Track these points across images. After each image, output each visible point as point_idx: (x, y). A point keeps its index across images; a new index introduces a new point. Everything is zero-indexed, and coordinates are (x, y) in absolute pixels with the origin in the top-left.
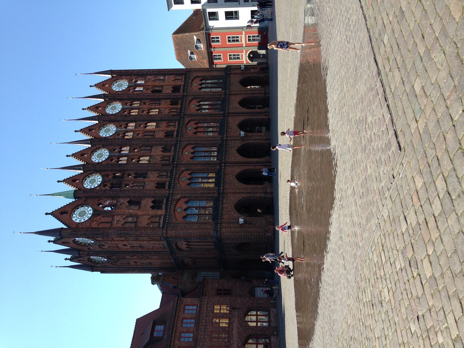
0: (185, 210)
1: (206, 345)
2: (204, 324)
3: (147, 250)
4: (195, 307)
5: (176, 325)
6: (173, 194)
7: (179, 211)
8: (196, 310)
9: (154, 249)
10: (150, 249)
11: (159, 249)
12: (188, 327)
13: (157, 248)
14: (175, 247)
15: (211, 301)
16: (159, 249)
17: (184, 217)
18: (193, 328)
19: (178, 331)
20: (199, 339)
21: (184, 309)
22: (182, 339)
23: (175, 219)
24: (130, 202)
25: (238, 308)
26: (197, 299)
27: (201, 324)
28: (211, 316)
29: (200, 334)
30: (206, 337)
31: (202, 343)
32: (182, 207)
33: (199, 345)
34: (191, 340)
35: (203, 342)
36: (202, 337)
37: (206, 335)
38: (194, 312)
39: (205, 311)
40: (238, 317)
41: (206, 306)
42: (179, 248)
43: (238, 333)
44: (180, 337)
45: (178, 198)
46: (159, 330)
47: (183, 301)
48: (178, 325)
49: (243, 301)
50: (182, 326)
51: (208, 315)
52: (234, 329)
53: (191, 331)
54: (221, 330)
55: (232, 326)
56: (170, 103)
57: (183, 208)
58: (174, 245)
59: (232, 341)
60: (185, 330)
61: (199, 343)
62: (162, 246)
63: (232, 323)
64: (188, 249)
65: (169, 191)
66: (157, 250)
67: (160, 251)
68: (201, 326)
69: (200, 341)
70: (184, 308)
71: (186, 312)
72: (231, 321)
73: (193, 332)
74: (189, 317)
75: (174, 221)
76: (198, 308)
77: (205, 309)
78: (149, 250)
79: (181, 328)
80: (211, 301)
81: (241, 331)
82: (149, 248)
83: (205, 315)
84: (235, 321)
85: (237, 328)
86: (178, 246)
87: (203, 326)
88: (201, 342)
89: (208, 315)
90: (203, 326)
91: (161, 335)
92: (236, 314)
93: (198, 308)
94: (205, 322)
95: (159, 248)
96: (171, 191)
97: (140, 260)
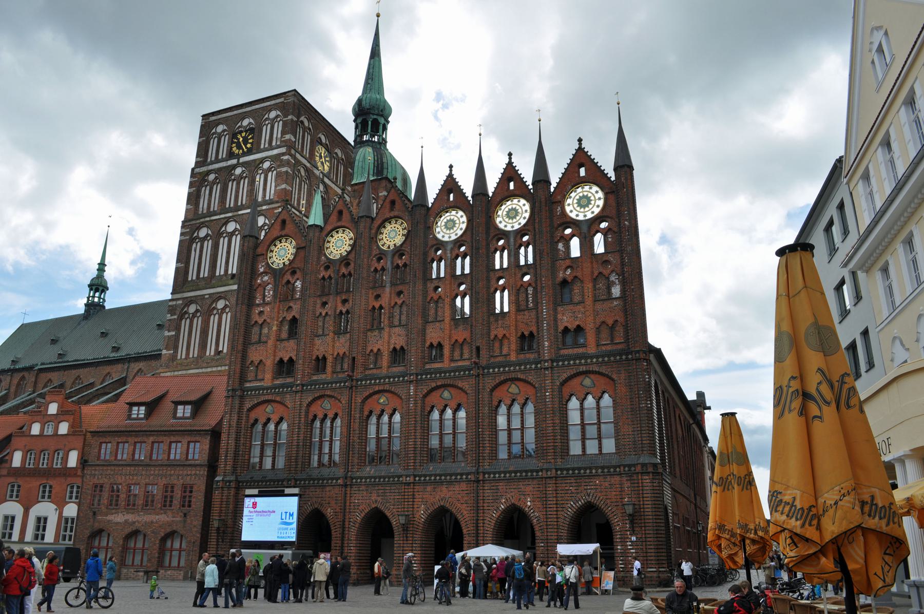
2: (169, 473)
4: (196, 457)
7: (267, 410)
15: (199, 479)
24: (294, 320)
25: (185, 521)
26: (207, 458)
27: (169, 469)
30: (152, 477)
33: (143, 470)
39: (185, 472)
40: (173, 521)
41: (194, 472)
44: (159, 442)
47: (206, 438)
48: (172, 437)
49: (195, 529)
51: (180, 477)
52: (157, 517)
55: (162, 514)
56: (526, 333)
59: (142, 513)
77: (189, 473)
80: (199, 479)
84: (168, 517)
92: (177, 519)
94: (171, 475)
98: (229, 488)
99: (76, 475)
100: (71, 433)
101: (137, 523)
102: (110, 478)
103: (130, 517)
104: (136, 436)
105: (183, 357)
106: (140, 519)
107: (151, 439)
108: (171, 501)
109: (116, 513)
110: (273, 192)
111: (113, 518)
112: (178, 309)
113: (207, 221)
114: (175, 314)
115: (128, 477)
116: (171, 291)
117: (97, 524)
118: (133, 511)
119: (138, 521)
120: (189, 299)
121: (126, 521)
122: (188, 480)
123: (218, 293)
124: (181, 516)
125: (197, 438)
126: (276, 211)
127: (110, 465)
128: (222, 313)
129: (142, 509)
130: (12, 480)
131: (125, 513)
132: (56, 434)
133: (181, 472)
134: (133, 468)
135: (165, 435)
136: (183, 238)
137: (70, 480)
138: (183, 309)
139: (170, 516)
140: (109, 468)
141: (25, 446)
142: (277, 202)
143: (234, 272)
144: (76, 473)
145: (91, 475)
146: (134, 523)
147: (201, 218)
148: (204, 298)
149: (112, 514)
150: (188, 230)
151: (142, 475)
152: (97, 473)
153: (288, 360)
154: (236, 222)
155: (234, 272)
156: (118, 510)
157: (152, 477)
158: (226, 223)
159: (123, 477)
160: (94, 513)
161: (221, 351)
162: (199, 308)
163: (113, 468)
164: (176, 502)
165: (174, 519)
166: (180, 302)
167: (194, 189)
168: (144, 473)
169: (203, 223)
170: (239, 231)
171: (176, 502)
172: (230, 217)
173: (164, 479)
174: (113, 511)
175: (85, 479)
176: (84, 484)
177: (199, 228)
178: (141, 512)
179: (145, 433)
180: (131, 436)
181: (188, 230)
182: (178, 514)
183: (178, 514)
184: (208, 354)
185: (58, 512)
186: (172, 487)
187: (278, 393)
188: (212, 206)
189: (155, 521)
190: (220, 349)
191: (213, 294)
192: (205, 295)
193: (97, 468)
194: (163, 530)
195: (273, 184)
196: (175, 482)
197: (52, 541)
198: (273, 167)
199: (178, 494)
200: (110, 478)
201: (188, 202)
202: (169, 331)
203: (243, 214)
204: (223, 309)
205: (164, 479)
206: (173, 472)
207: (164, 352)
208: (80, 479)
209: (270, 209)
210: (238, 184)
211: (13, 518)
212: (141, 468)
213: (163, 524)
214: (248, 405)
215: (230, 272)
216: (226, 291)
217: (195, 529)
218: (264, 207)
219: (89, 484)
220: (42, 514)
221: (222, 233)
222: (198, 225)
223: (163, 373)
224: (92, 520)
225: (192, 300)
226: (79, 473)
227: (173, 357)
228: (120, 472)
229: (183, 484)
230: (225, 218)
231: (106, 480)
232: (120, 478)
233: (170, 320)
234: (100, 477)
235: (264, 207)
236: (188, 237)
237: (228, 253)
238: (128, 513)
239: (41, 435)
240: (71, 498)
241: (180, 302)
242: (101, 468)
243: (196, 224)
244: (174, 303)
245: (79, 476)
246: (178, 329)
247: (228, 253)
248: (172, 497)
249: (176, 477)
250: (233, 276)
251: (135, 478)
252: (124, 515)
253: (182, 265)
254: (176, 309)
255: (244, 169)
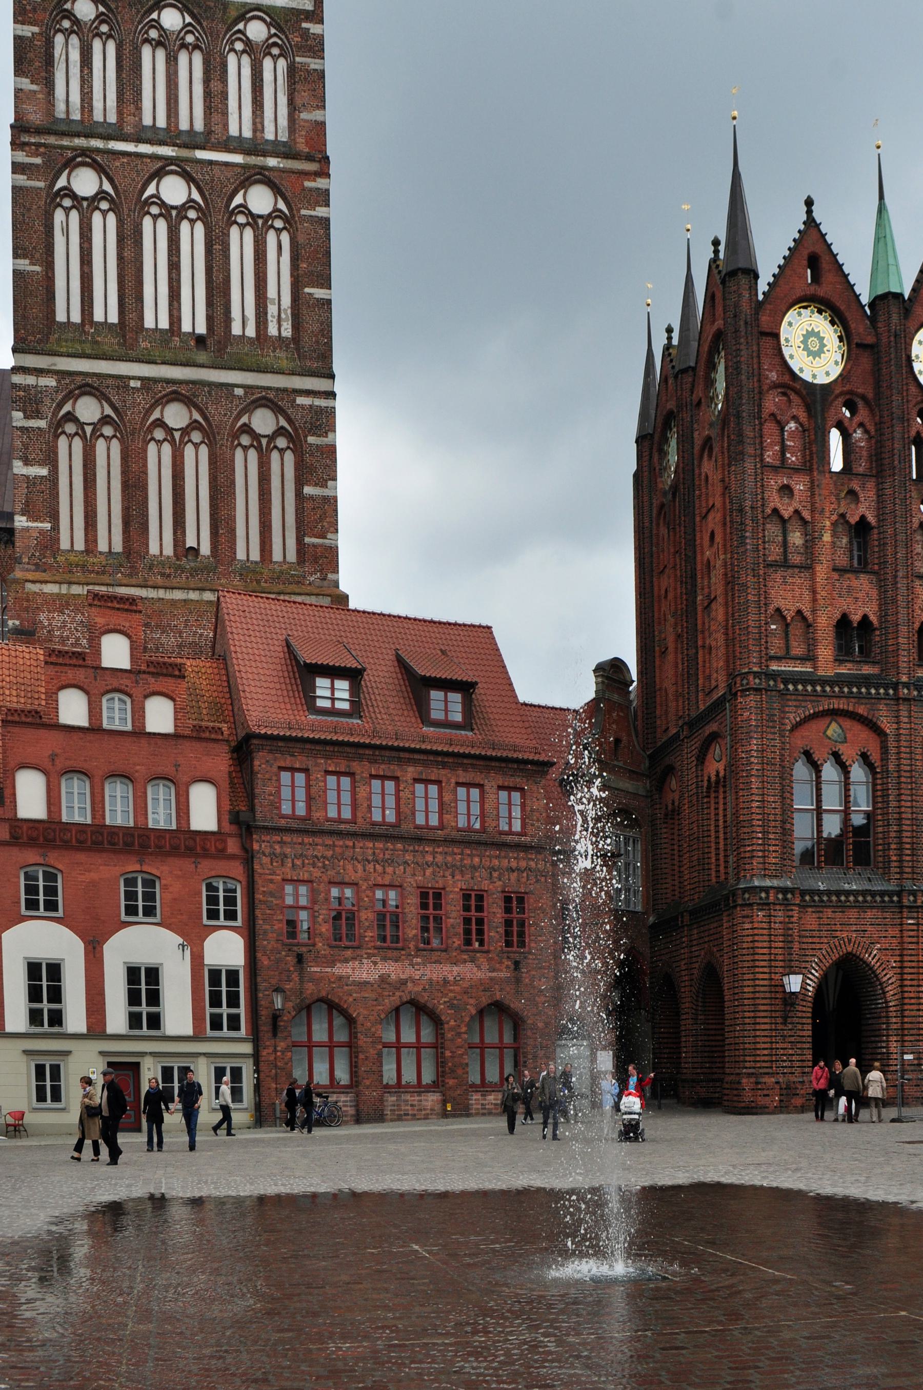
0: (836, 756)
1: (404, 873)
3: (699, 627)
5: (462, 764)
6: (897, 699)
8: (510, 833)
9: (704, 654)
10: (704, 638)
11: (704, 672)
12: (456, 807)
13: (707, 665)
14: (707, 733)
16: (704, 672)
17: (808, 754)
18: (453, 824)
19: (443, 772)
20: (421, 848)
21: (509, 789)
22: (420, 788)
23: (798, 719)
28: (491, 887)
29: (436, 850)
30: (429, 871)
31: (412, 858)
32: (845, 741)
34: (420, 820)
35: (413, 862)
36: (429, 858)
37: (433, 873)
38: (504, 827)
40: (491, 979)
42: (707, 749)
43: (446, 981)
44: (427, 782)
45: (879, 723)
46: (451, 706)
48: (460, 772)
50: (459, 784)
52: (455, 968)
53: (446, 817)
54: (452, 920)
55: (465, 961)
57: (842, 749)
58: (713, 727)
59: (419, 960)
60: (447, 798)
61: (411, 848)
62: (714, 684)
63: (473, 960)
64: (705, 784)
65: (906, 685)
66: (701, 663)
67: (697, 680)
68: (462, 854)
69: (417, 851)
70: (516, 789)
71: (503, 795)
72: (478, 955)
73: (441, 827)
74: (486, 806)
75: (792, 716)
76: (516, 838)
78: (700, 636)
79: (453, 781)
81: (451, 991)
82: (707, 633)
83: (496, 862)
85: (458, 978)
86: (713, 744)
87: (462, 860)
88: (414, 856)
89: (495, 874)
90: (462, 860)
91: (436, 714)
92: (502, 975)
93: (516, 838)
94: (474, 868)
95: (707, 671)
96: (906, 691)
97: (673, 608)
98: (786, 904)
99: (221, 854)
100: (187, 732)
101: (409, 984)
102: (324, 866)
103: (392, 970)
104: (373, 761)
105: (80, 545)
106: (417, 975)
107: (411, 771)
108: (508, 933)
109: (354, 959)
110: (283, 121)
111: (350, 971)
112: (47, 401)
113: (98, 150)
114: (37, 415)
115: (370, 867)
116: (10, 342)
117: (310, 988)
118: (396, 953)
119: (413, 981)
120: (79, 380)
121: (383, 979)
122: (513, 882)
123: (169, 381)
124: (508, 967)
125: (518, 781)
126: (307, 184)
127: (322, 832)
128: (183, 443)
129: (418, 950)
130: (31, 856)
131: (378, 959)
132: (139, 733)
133: (496, 862)
134: (379, 845)
135: (444, 765)
136: (22, 180)
137: (207, 867)
138: (60, 406)
139: (485, 966)
140: (318, 840)
141: (53, 758)
142: (309, 158)
143: (201, 329)
144: (224, 850)
145: (273, 855)
146: (404, 982)
147: (78, 135)
148: (127, 387)
149: (346, 961)
150: (38, 161)
151: (406, 863)
152: (288, 850)
153: (859, 623)
154: (188, 178)
155: (201, 329)
156: (358, 952)
157: (429, 871)
158: (159, 174)
159: (360, 867)
160: (300, 959)
161: (195, 551)
162: (108, 411)
163: (329, 841)
164: (494, 933)
165: (494, 974)
166: (51, 382)
167: (36, 29)
168: (408, 857)
169: (84, 152)
170: (198, 208)
171: (494, 933)
172: (169, 160)
173: (458, 877)
174: (349, 953)
175: (256, 866)
176: (259, 881)
177: (71, 164)
178: (417, 956)
179: (394, 754)
180: (361, 758)
181: (38, 161)
182: (501, 963)
183: (501, 963)
184: (154, 549)
185: (188, 953)
186: (480, 898)
187: (859, 697)
188: (98, 104)
189: (451, 978)
190: (191, 542)
191: (155, 380)
192: (134, 378)
193: (287, 838)
194: (472, 1001)
195: (283, 100)
196: (485, 885)
197: (189, 1031)
198: (275, 44)
199: (495, 913)
200: (324, 866)
201: (21, 65)
202: (27, 462)
203: (211, 163)
204: (185, 431)
205: (458, 877)
206: (476, 860)
207: (20, 522)
208: (237, 869)
209: (292, 172)
210: (171, 61)
211: (55, 970)
212: (399, 846)
213: (471, 987)
214: (793, 717)
215: (186, 327)
216: (193, 382)
217: (543, 999)
218: (272, 162)
219: (271, 881)
220: (143, 958)
221: (148, 203)
222: (70, 154)
223: (33, 582)
224: (295, 976)
225: (88, 385)
226: (233, 847)
227: (50, 541)
228: (348, 853)
229: (503, 892)
230: (154, 157)
231: (317, 873)
232: (349, 867)
233: (22, 429)
234: (298, 862)
235: (272, 162)
236: (41, 184)
237: (174, 266)
238: (385, 959)
239: (95, 729)
240: (213, 915)
241: (51, 382)
242: (297, 839)
243: (62, 147)
244: (30, 380)
245: (233, 857)
246: (51, 460)
247: (174, 266)
248: (480, 922)
249: (484, 873)
250: (200, 341)
251: (389, 870)
252: (375, 963)
253: (37, 268)
254: (39, 402)
255: (188, 19)
